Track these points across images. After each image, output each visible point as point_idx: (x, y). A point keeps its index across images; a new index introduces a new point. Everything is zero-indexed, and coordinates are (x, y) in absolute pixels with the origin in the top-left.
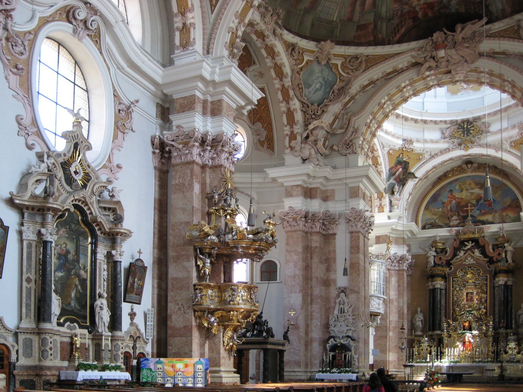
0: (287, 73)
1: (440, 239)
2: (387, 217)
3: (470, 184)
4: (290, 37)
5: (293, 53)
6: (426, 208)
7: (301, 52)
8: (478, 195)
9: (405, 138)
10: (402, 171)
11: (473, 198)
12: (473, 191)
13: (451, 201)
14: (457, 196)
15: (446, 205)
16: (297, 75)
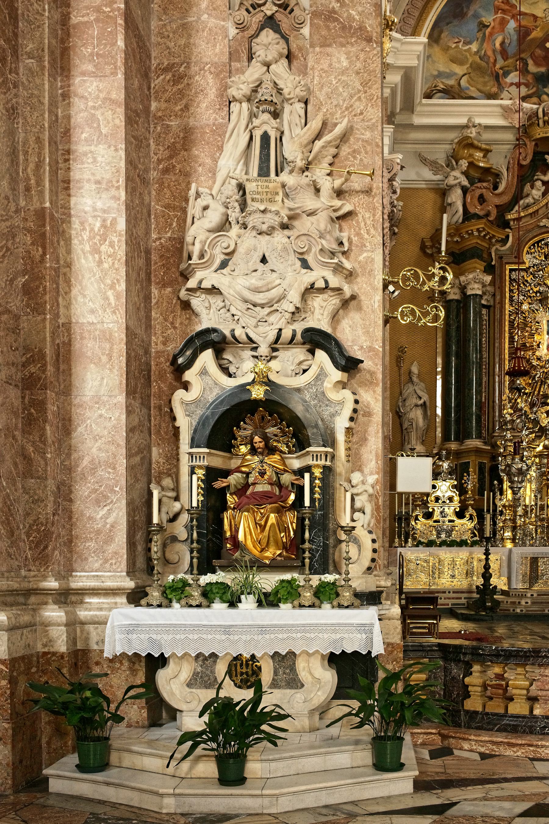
13: (503, 23)
15: (491, 34)
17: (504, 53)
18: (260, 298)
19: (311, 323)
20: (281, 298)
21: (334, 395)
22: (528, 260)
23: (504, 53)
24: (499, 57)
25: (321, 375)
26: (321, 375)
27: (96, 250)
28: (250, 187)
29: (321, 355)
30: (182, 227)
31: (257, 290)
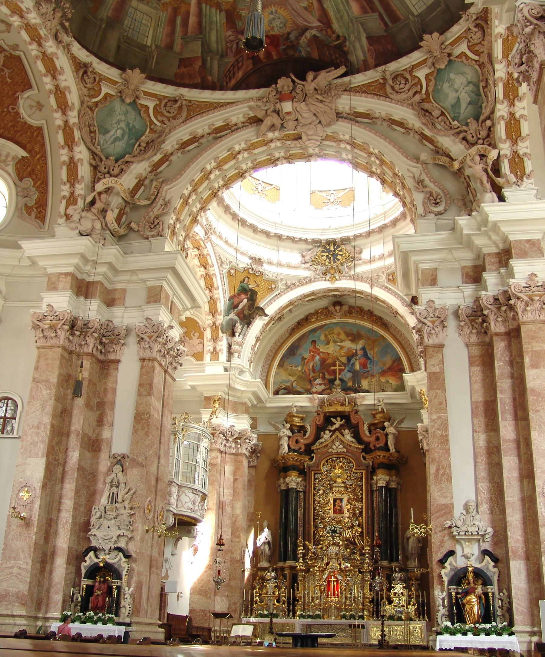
0: (73, 104)
1: (297, 412)
2: (223, 370)
3: (339, 334)
4: (83, 55)
5: (86, 78)
6: (281, 365)
7: (97, 79)
8: (349, 350)
9: (252, 256)
10: (246, 303)
11: (343, 354)
12: (343, 344)
13: (313, 357)
14: (321, 350)
15: (308, 362)
16: (90, 112)
17: (314, 371)
18: (106, 538)
19: (119, 545)
20: (112, 538)
21: (123, 565)
22: (324, 469)
23: (314, 371)
24: (311, 372)
25: (120, 559)
26: (120, 559)
27: (64, 527)
28: (107, 507)
29: (121, 554)
30: (90, 518)
31: (105, 536)
